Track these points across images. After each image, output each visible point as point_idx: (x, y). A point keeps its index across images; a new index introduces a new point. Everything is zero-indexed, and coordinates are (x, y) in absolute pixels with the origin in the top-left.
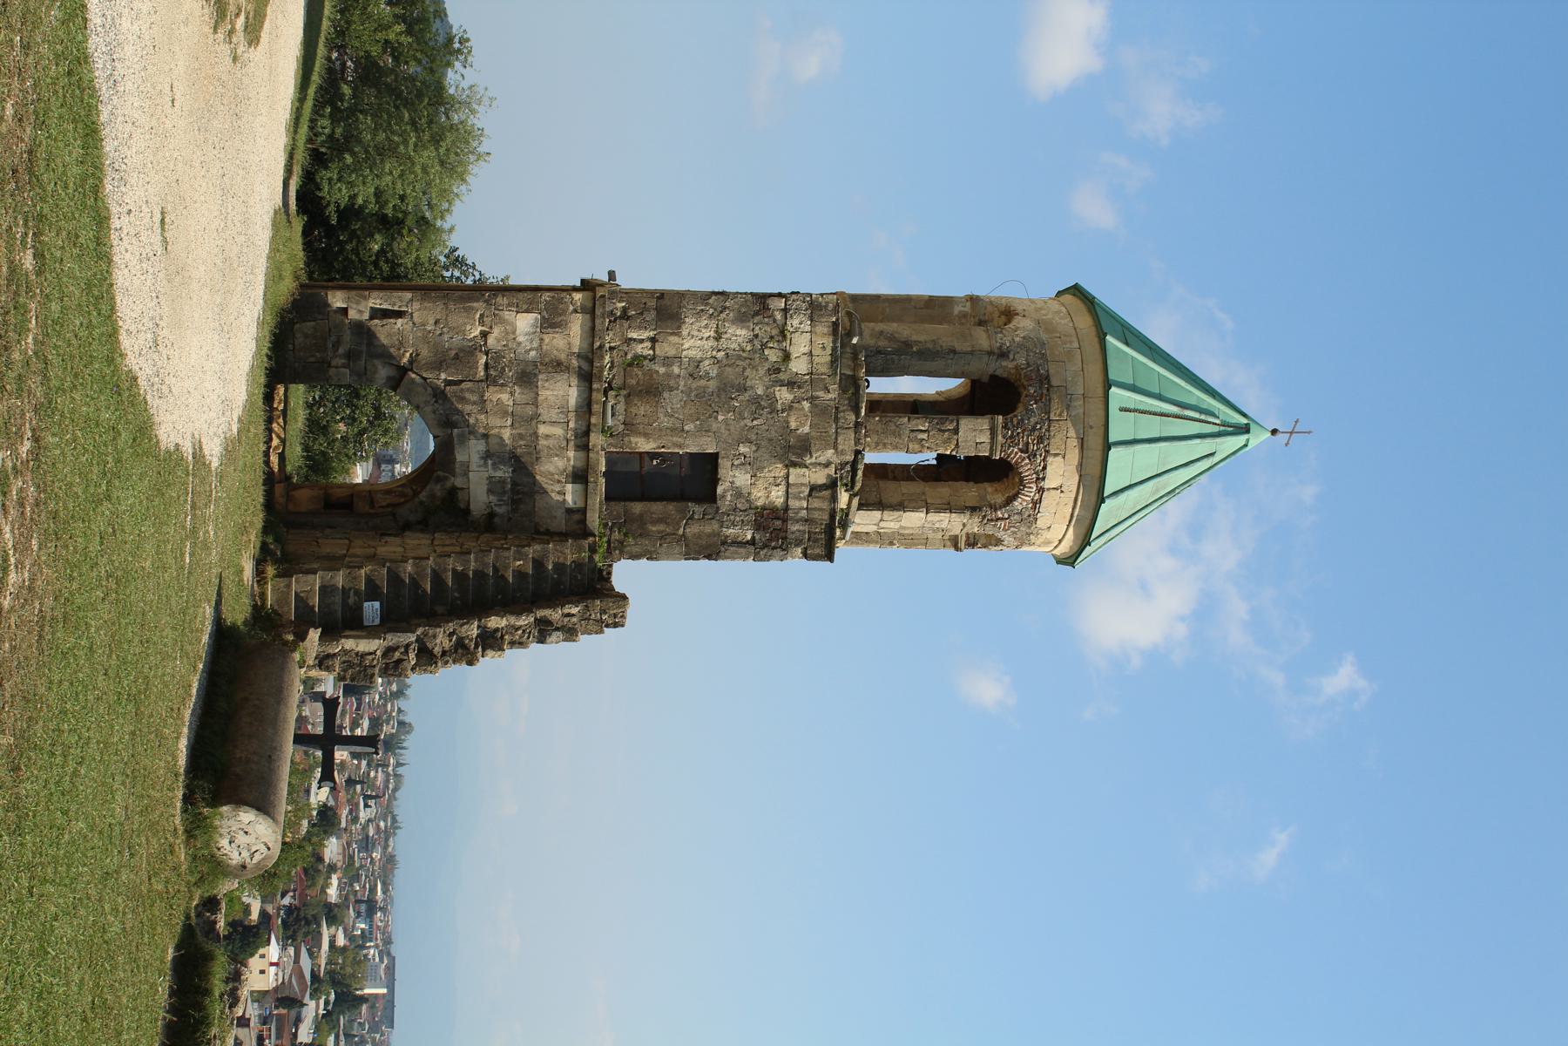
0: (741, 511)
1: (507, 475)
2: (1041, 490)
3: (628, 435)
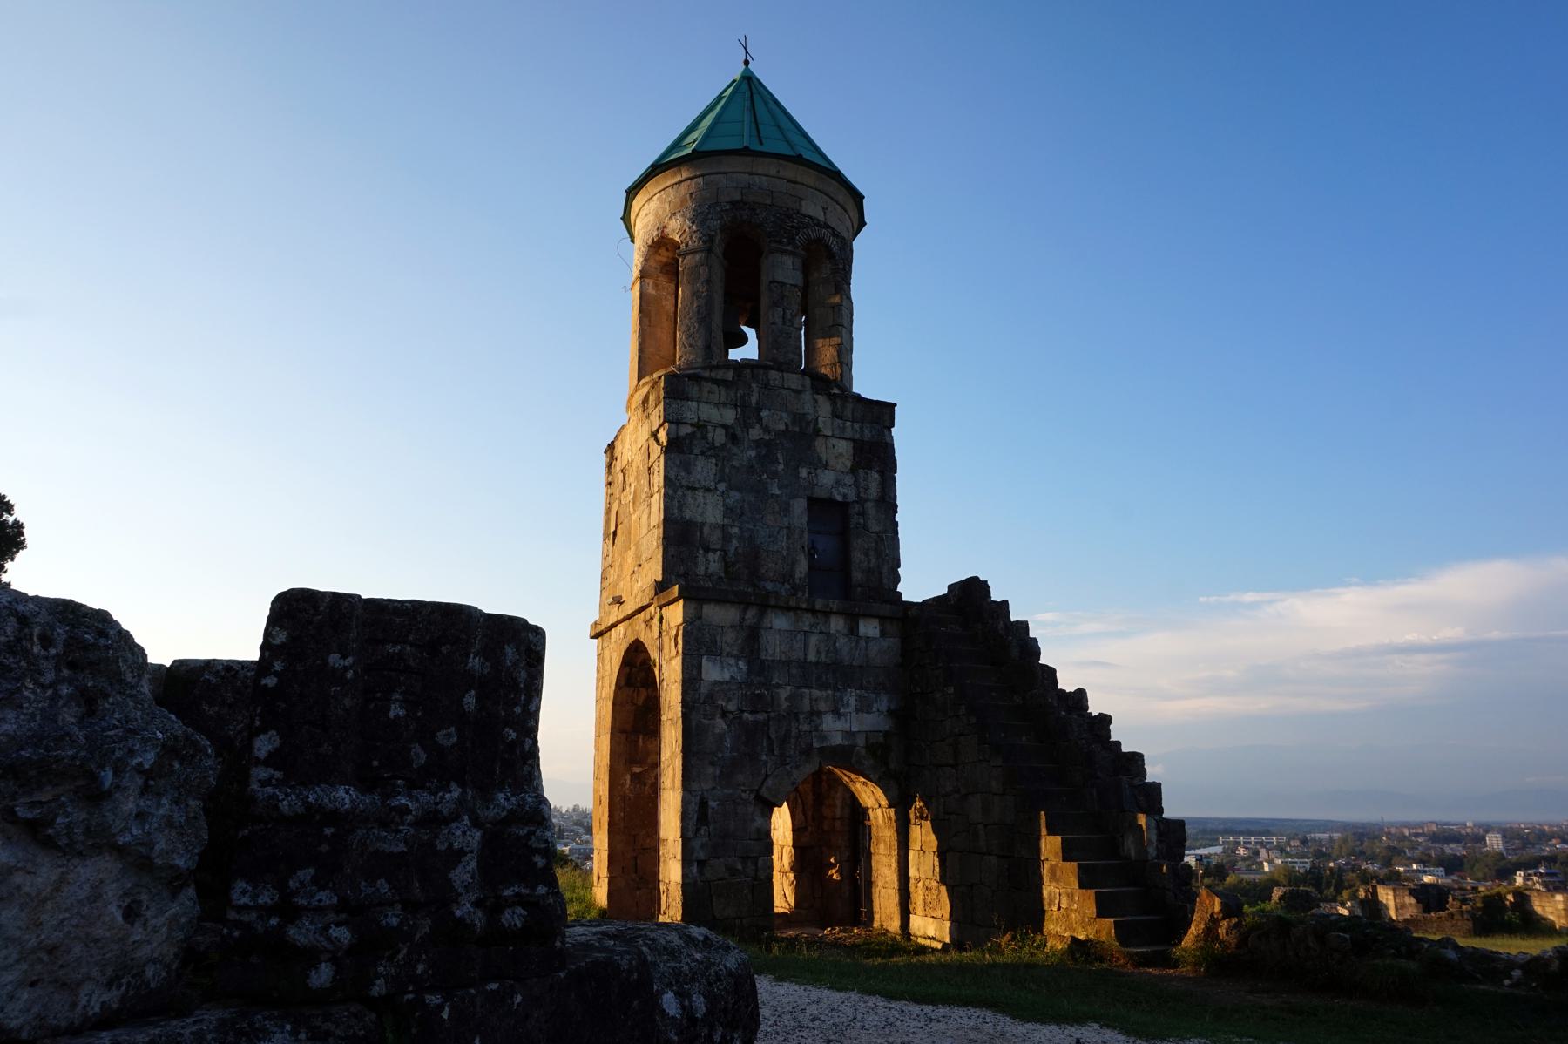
1: (853, 694)
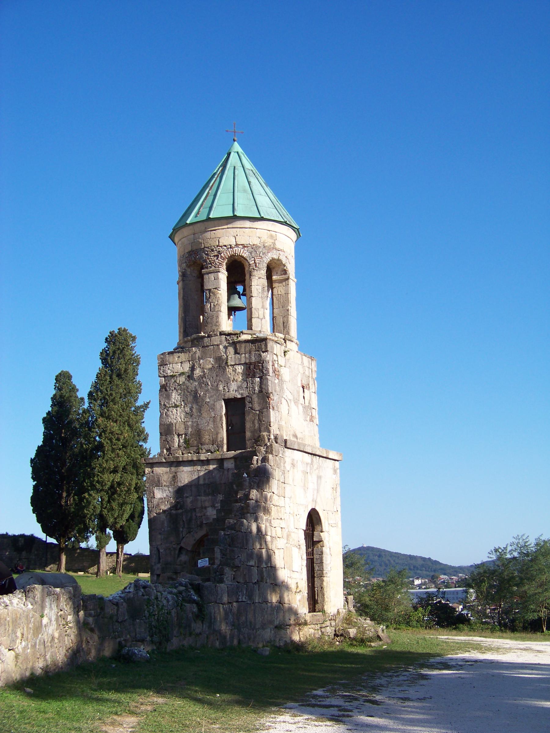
0: (247, 385)
2: (237, 245)
3: (217, 442)
